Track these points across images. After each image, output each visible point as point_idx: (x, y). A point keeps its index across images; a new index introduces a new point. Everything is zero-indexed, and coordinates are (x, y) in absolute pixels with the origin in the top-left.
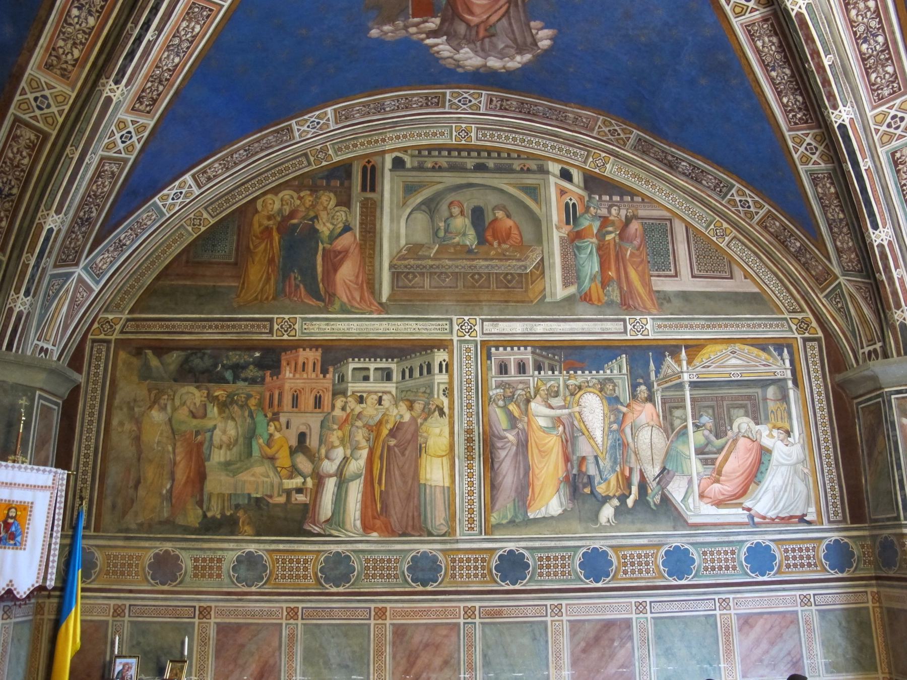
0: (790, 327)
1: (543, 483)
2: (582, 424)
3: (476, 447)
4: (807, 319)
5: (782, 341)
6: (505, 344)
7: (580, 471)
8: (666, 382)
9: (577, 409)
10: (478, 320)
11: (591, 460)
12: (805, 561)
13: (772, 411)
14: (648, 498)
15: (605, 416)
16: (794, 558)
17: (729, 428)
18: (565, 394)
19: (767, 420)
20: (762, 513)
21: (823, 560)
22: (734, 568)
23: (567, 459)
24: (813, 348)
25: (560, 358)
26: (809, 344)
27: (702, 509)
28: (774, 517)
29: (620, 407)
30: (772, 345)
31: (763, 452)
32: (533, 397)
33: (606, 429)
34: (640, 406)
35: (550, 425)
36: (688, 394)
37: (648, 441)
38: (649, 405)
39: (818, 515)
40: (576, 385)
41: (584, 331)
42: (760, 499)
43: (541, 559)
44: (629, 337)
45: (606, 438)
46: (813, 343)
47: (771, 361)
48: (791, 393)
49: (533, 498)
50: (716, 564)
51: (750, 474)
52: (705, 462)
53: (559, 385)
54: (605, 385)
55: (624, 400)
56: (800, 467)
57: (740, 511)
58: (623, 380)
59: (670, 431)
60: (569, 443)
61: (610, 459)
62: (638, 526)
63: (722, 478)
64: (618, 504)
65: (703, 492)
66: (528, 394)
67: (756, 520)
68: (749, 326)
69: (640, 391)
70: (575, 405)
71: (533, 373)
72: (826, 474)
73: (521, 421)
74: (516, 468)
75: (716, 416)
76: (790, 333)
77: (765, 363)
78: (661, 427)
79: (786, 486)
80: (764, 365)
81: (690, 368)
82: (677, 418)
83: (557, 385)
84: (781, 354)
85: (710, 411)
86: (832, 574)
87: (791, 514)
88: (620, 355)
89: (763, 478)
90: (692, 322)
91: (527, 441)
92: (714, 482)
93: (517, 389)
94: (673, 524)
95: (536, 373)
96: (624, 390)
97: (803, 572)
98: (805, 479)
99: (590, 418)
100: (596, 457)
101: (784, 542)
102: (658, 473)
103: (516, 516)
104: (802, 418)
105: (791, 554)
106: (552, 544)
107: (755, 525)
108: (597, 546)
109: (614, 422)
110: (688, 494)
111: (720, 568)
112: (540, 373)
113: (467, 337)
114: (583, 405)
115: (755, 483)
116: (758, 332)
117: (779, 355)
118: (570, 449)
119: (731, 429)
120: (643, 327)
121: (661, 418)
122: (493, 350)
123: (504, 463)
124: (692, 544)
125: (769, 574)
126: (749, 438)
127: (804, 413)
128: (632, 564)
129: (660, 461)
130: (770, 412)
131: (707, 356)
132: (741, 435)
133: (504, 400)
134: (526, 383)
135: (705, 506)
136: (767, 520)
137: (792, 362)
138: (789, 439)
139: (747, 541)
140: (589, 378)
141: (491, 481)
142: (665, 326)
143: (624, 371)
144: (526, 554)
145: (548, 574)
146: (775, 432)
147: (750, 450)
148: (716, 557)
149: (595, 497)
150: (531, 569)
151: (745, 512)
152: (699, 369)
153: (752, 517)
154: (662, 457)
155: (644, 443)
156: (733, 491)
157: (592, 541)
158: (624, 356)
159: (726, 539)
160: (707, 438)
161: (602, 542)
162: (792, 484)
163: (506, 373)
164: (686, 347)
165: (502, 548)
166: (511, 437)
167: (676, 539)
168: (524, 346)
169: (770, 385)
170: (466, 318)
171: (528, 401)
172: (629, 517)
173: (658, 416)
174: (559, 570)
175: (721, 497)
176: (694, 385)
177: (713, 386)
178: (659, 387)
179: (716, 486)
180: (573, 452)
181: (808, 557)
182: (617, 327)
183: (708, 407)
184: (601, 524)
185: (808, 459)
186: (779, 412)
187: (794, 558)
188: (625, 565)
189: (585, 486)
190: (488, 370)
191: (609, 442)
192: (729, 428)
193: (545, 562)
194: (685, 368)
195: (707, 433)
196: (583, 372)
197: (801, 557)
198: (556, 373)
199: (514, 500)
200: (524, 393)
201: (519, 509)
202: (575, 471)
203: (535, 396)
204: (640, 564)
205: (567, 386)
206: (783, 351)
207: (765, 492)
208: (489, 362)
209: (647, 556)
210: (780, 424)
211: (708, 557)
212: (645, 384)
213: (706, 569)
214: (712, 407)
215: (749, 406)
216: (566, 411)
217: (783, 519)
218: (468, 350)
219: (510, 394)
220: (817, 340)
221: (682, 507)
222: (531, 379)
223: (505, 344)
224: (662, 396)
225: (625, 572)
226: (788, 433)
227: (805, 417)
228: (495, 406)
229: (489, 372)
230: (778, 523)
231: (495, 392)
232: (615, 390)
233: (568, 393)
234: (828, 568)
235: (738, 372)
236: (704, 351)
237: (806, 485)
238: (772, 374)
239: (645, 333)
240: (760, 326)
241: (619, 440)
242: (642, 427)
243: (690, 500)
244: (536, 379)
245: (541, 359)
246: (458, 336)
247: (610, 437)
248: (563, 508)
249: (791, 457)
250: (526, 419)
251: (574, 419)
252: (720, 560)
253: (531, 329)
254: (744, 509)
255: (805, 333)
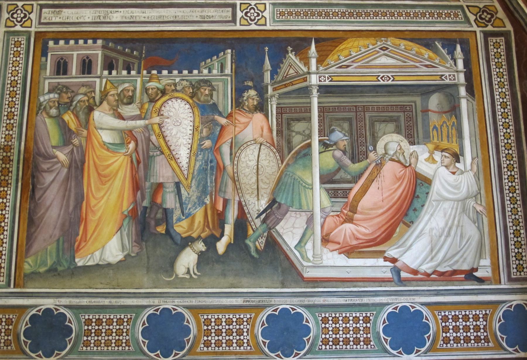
0: (466, 16)
1: (100, 217)
2: (161, 140)
3: (14, 169)
4: (490, 8)
5: (454, 36)
6: (67, 37)
7: (153, 201)
8: (286, 86)
9: (156, 120)
10: (35, 5)
11: (170, 188)
12: (472, 334)
13: (435, 127)
14: (247, 242)
15: (195, 129)
16: (456, 329)
17: (371, 148)
18: (142, 100)
19: (427, 138)
20: (413, 266)
21: (498, 334)
22: (367, 341)
23: (136, 186)
24: (497, 45)
25: (141, 54)
26: (492, 40)
27: (324, 257)
28: (429, 271)
29: (217, 117)
30: (441, 40)
31: (419, 181)
32: (98, 103)
33: (195, 146)
34: (247, 117)
35: (118, 141)
36: (315, 101)
37: (254, 163)
38: (259, 117)
39: (493, 271)
40: (158, 89)
41: (177, 19)
42: (411, 245)
43: (88, 322)
44: (238, 27)
45: (193, 158)
46: (498, 39)
47: (437, 61)
48: (464, 104)
49: (85, 238)
50: (341, 336)
51: (398, 210)
52: (334, 194)
53: (135, 89)
54: (199, 89)
55: (224, 107)
56: (471, 203)
57: (381, 262)
58: (225, 82)
59: (286, 151)
60: (141, 165)
61: (198, 187)
62: (231, 279)
63: (356, 216)
64: (203, 249)
65: (328, 235)
66: (91, 101)
67: (404, 275)
68: (408, 15)
69: (248, 97)
70: (154, 115)
71: (102, 73)
72: (508, 214)
73: (78, 134)
74: (65, 197)
75: (355, 133)
76: (467, 25)
77: (428, 63)
78: (274, 147)
79: (450, 228)
80: (427, 66)
81: (321, 68)
82: (298, 133)
83: (132, 88)
84: (451, 53)
85: (346, 125)
86: (511, 353)
87: (455, 267)
88: (224, 51)
89: (417, 217)
90: (329, 9)
91: (83, 163)
92: (345, 221)
93: (77, 94)
94: (281, 279)
95: (106, 73)
96: (225, 95)
97: (468, 349)
98: (477, 221)
99: (174, 132)
100: (178, 185)
101: (443, 307)
102: (264, 207)
103: (58, 262)
104: (478, 137)
105: (451, 324)
106: (106, 302)
107: (402, 282)
108: (170, 307)
109: (208, 138)
110: (307, 237)
111: (347, 342)
112: (110, 73)
113: (18, 28)
114: (166, 114)
115: (405, 224)
116: (421, 22)
117: (448, 54)
118: (142, 173)
119: (375, 149)
120: (258, 15)
121: (275, 133)
122: (51, 43)
123: (48, 191)
124: (307, 307)
125: (418, 351)
126: (399, 162)
127: (480, 131)
128: (219, 333)
129: (269, 191)
130: (431, 128)
131: (346, 52)
132: (387, 157)
133: (58, 108)
134: (91, 86)
135: (330, 254)
136: (419, 276)
137: (467, 63)
138: (457, 165)
139: (388, 304)
140: (178, 80)
141: (29, 213)
142: (290, 14)
143: (228, 71)
144: (69, 314)
145: (98, 344)
146: (438, 156)
147: (399, 179)
148: (341, 325)
149: (172, 238)
150: (73, 335)
151: (388, 264)
152: (333, 69)
153: (397, 271)
154: (272, 185)
155: (248, 167)
156: (372, 234)
157: (162, 300)
158: (229, 51)
159: (357, 301)
160: (338, 161)
161: (177, 301)
162: (458, 226)
163: (65, 73)
164: (317, 41)
165: (36, 306)
166: (62, 156)
167: (283, 299)
168: (93, 39)
169: (434, 92)
170: (20, 4)
171: (90, 109)
172: (218, 267)
173: (271, 130)
174: (114, 338)
175: (354, 242)
176: (324, 90)
177: (352, 92)
178: (275, 92)
179: (348, 226)
180: (146, 178)
181: (477, 329)
182: (224, 14)
183: (344, 119)
184: (177, 275)
185: (483, 192)
186: (445, 129)
187: (456, 329)
188: (208, 333)
189: (158, 224)
190: (41, 69)
191: (198, 164)
192: (371, 148)
193: (94, 327)
194: (313, 68)
195: (338, 154)
196: (170, 72)
197: (467, 329)
198: (133, 73)
199: (58, 240)
200: (86, 98)
201: (63, 253)
202: (146, 203)
203: (101, 103)
204: (229, 332)
205: (147, 90)
206: (455, 49)
207: (418, 237)
208: (43, 59)
209: (240, 321)
210: (445, 144)
211: (330, 326)
212: (255, 88)
213: (325, 342)
214: (349, 120)
215: (402, 119)
216: (141, 123)
217: (442, 274)
218: (18, 44)
219: (67, 101)
220: (505, 34)
221: (295, 255)
222: (98, 80)
223: (67, 35)
224: (278, 104)
225: (207, 344)
226: (457, 157)
227: (481, 134)
228: (45, 115)
229: (43, 72)
230: (434, 280)
231: (47, 97)
232: (211, 96)
233: (146, 99)
234: (504, 344)
235: (389, 75)
236: (342, 47)
237: (478, 228)
238: (438, 78)
239: (262, 22)
240: (424, 15)
241: (211, 162)
242: (247, 144)
243: (309, 246)
244: (104, 80)
245: (113, 55)
246: (6, 26)
247: (200, 157)
248: (125, 253)
249: (458, 189)
250: (85, 133)
251: (152, 133)
252: (346, 330)
253: (104, 17)
254: (386, 259)
255: (487, 26)
